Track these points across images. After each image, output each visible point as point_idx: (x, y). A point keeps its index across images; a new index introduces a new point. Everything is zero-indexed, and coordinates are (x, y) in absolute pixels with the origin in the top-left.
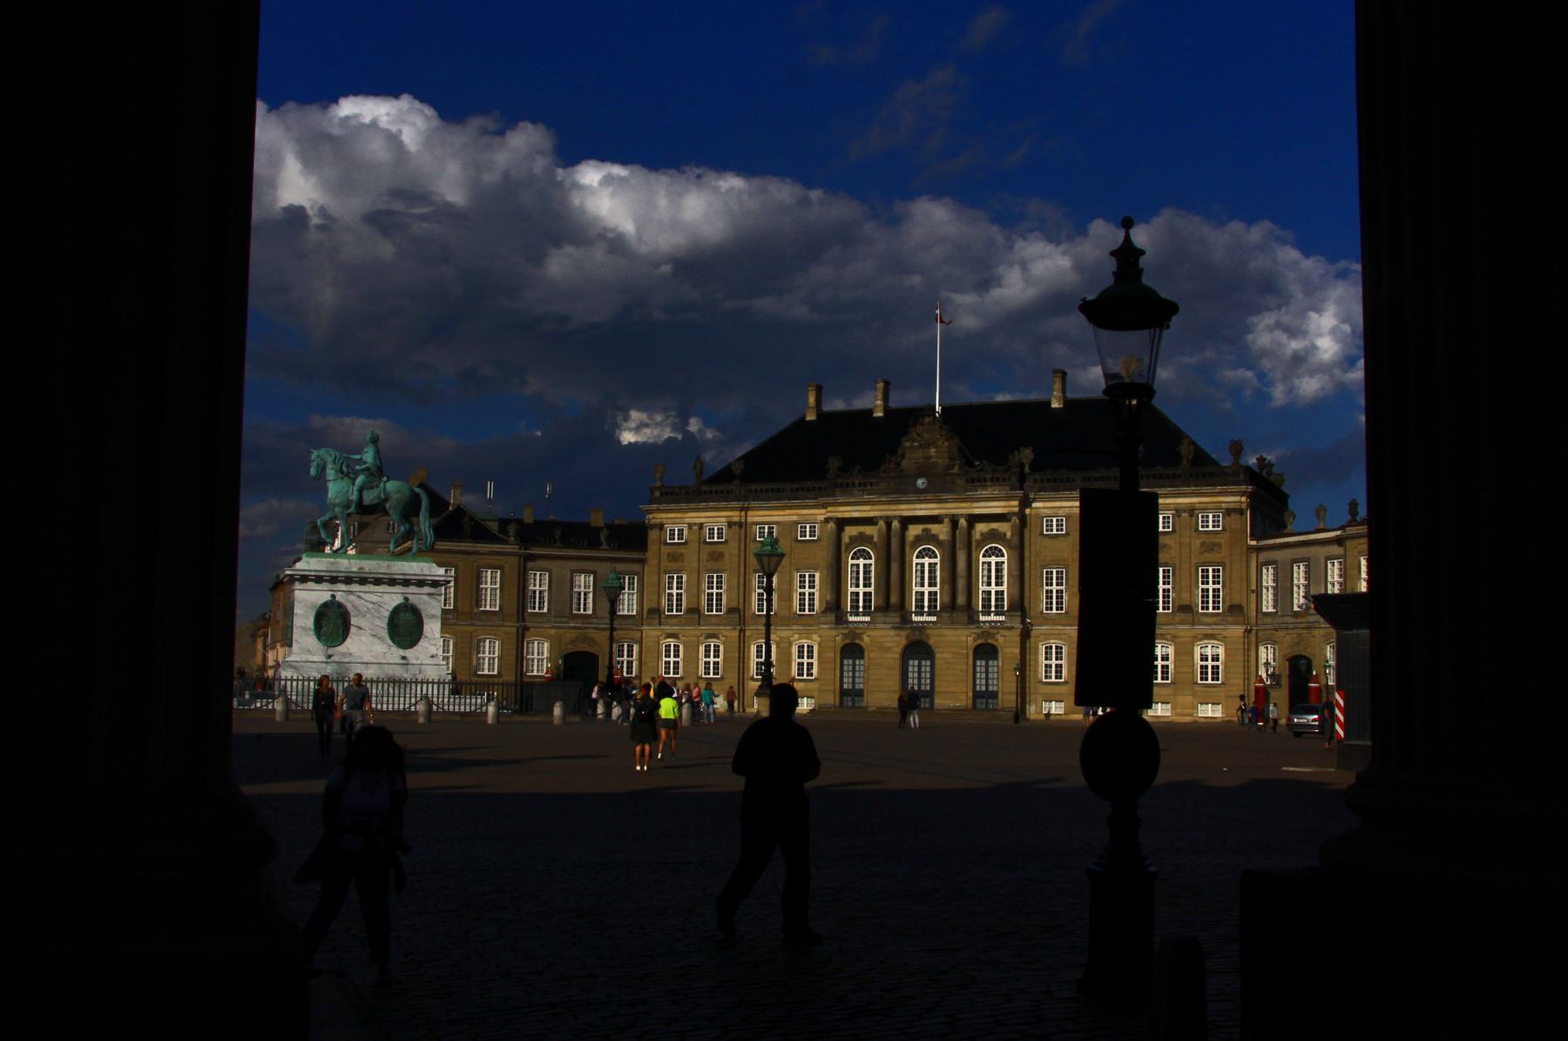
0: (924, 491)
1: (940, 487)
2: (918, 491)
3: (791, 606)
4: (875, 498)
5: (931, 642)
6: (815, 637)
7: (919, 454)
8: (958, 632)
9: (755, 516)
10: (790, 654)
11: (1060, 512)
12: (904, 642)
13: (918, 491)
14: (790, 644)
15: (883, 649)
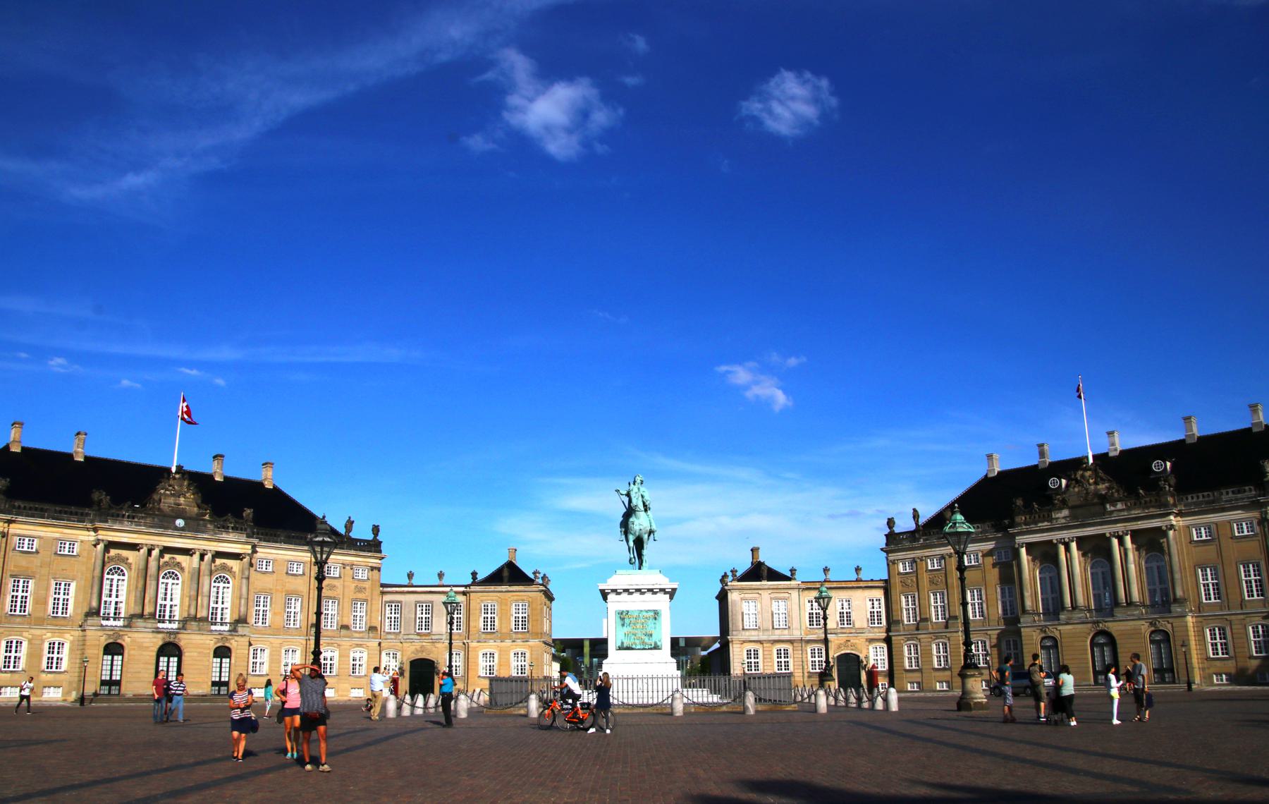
0: (182, 529)
1: (194, 526)
2: (177, 529)
3: (46, 610)
4: (143, 528)
5: (182, 644)
6: (68, 636)
7: (172, 500)
8: (204, 637)
9: (15, 529)
10: (42, 650)
11: (270, 557)
12: (160, 643)
13: (177, 529)
14: (43, 641)
15: (141, 647)
